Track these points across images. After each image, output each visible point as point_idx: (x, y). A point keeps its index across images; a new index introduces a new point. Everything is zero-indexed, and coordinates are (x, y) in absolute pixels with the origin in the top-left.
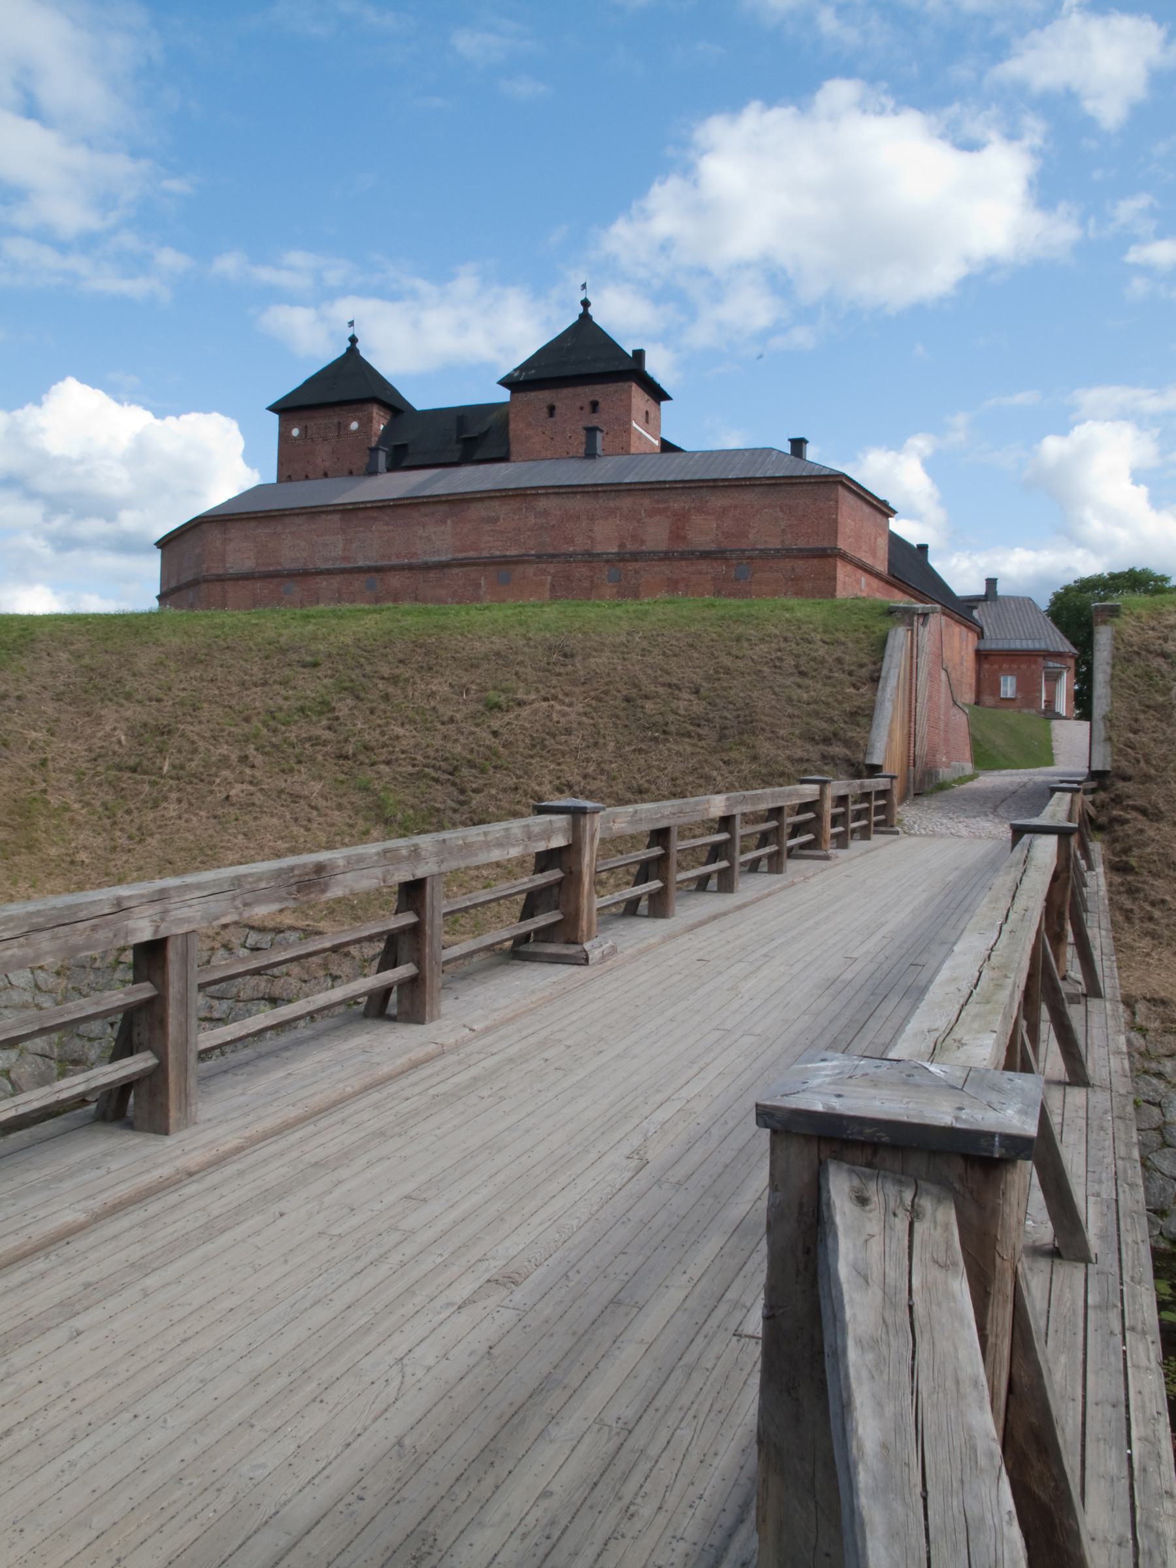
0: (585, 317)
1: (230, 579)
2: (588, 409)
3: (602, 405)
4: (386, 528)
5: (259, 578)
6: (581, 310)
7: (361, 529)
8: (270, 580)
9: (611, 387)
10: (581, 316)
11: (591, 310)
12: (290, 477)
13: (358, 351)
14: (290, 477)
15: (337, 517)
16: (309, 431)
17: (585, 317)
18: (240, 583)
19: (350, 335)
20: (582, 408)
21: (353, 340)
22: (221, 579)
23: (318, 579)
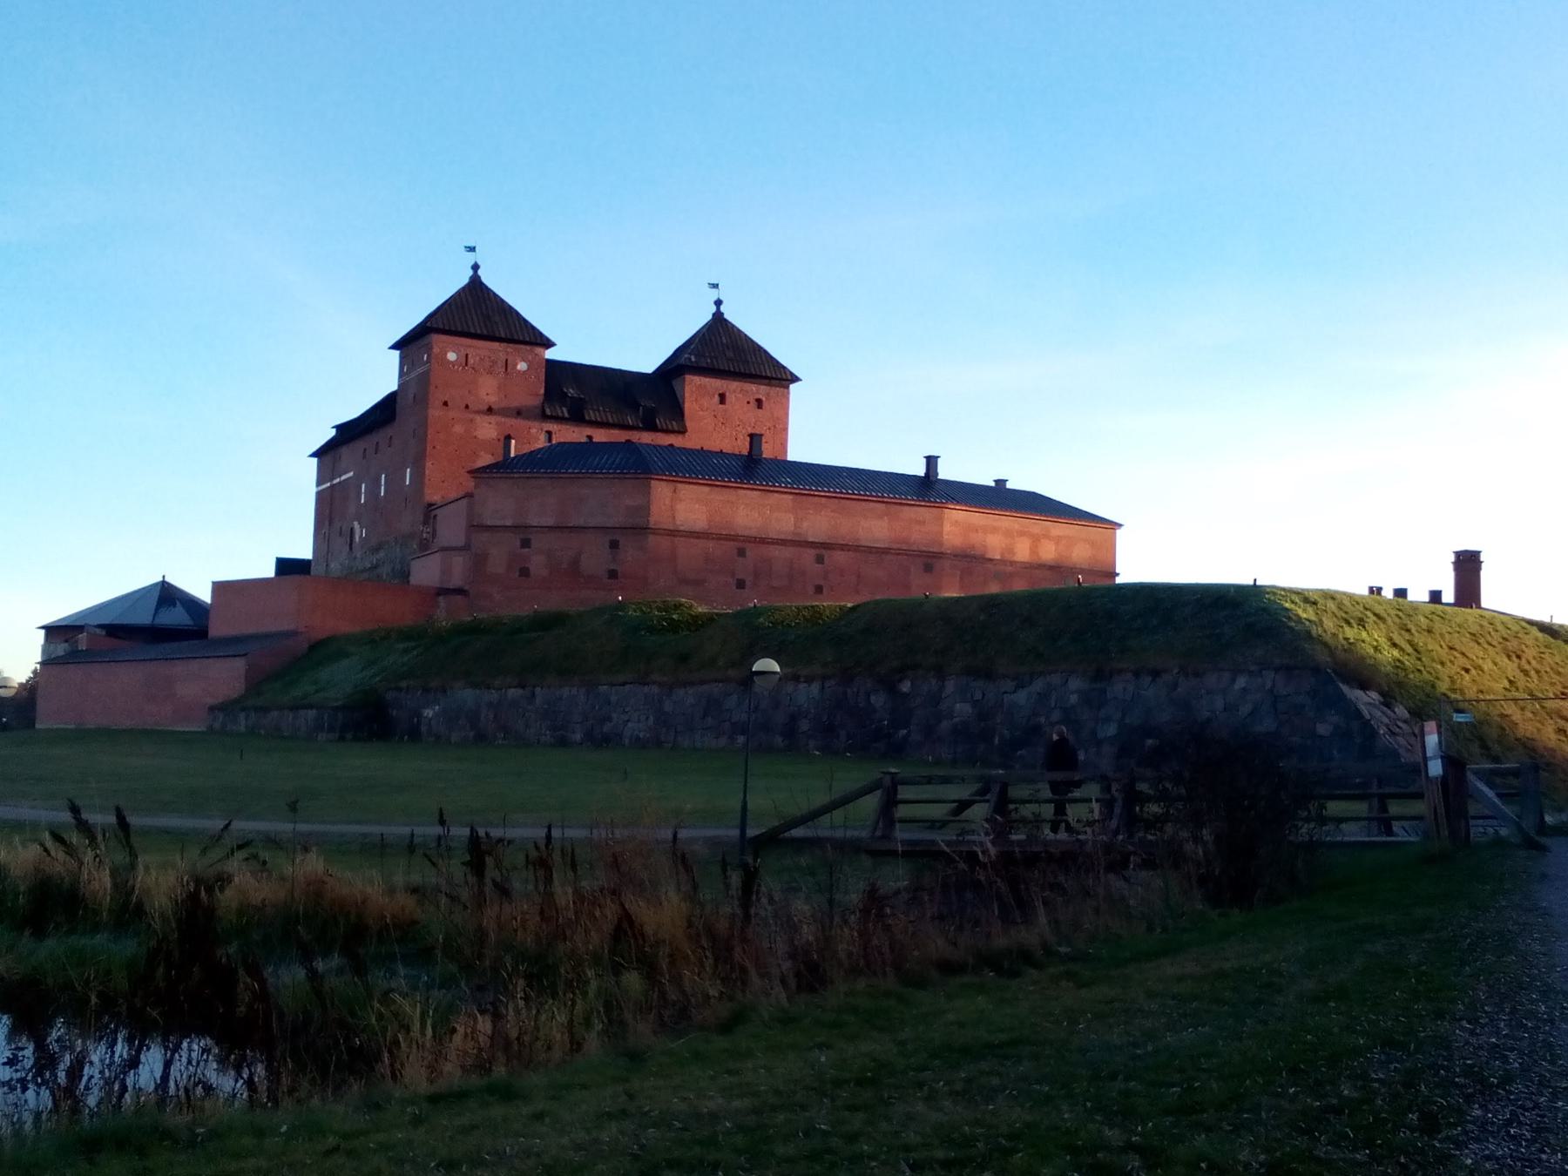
0: (718, 318)
1: (681, 536)
2: (753, 404)
3: (765, 404)
4: (832, 514)
5: (713, 539)
6: (714, 309)
7: (811, 512)
8: (722, 542)
9: (774, 391)
10: (714, 315)
11: (722, 308)
12: (445, 404)
13: (479, 277)
14: (445, 404)
15: (791, 497)
16: (471, 361)
17: (718, 318)
18: (692, 540)
19: (473, 263)
20: (748, 403)
21: (476, 267)
22: (673, 533)
23: (772, 547)
